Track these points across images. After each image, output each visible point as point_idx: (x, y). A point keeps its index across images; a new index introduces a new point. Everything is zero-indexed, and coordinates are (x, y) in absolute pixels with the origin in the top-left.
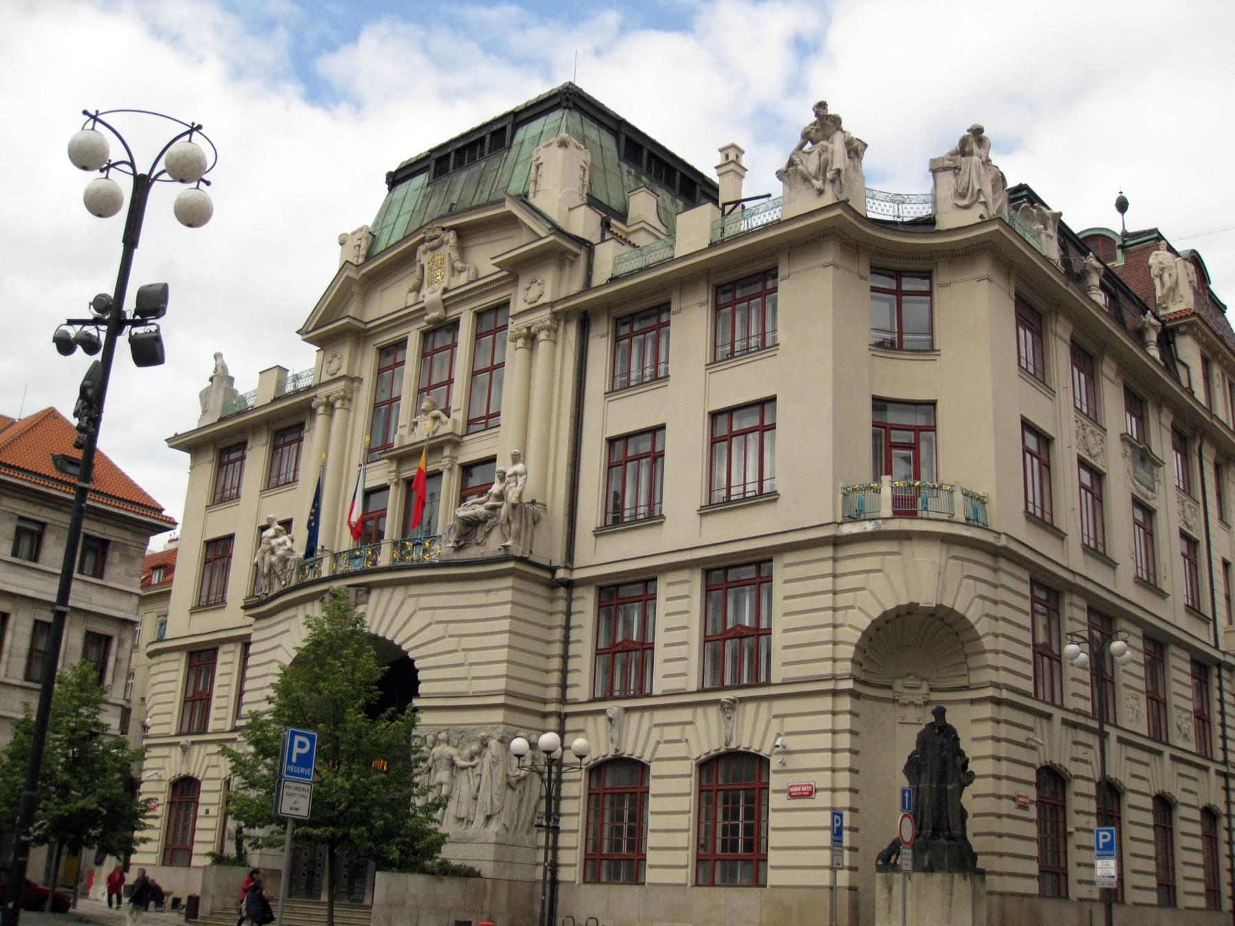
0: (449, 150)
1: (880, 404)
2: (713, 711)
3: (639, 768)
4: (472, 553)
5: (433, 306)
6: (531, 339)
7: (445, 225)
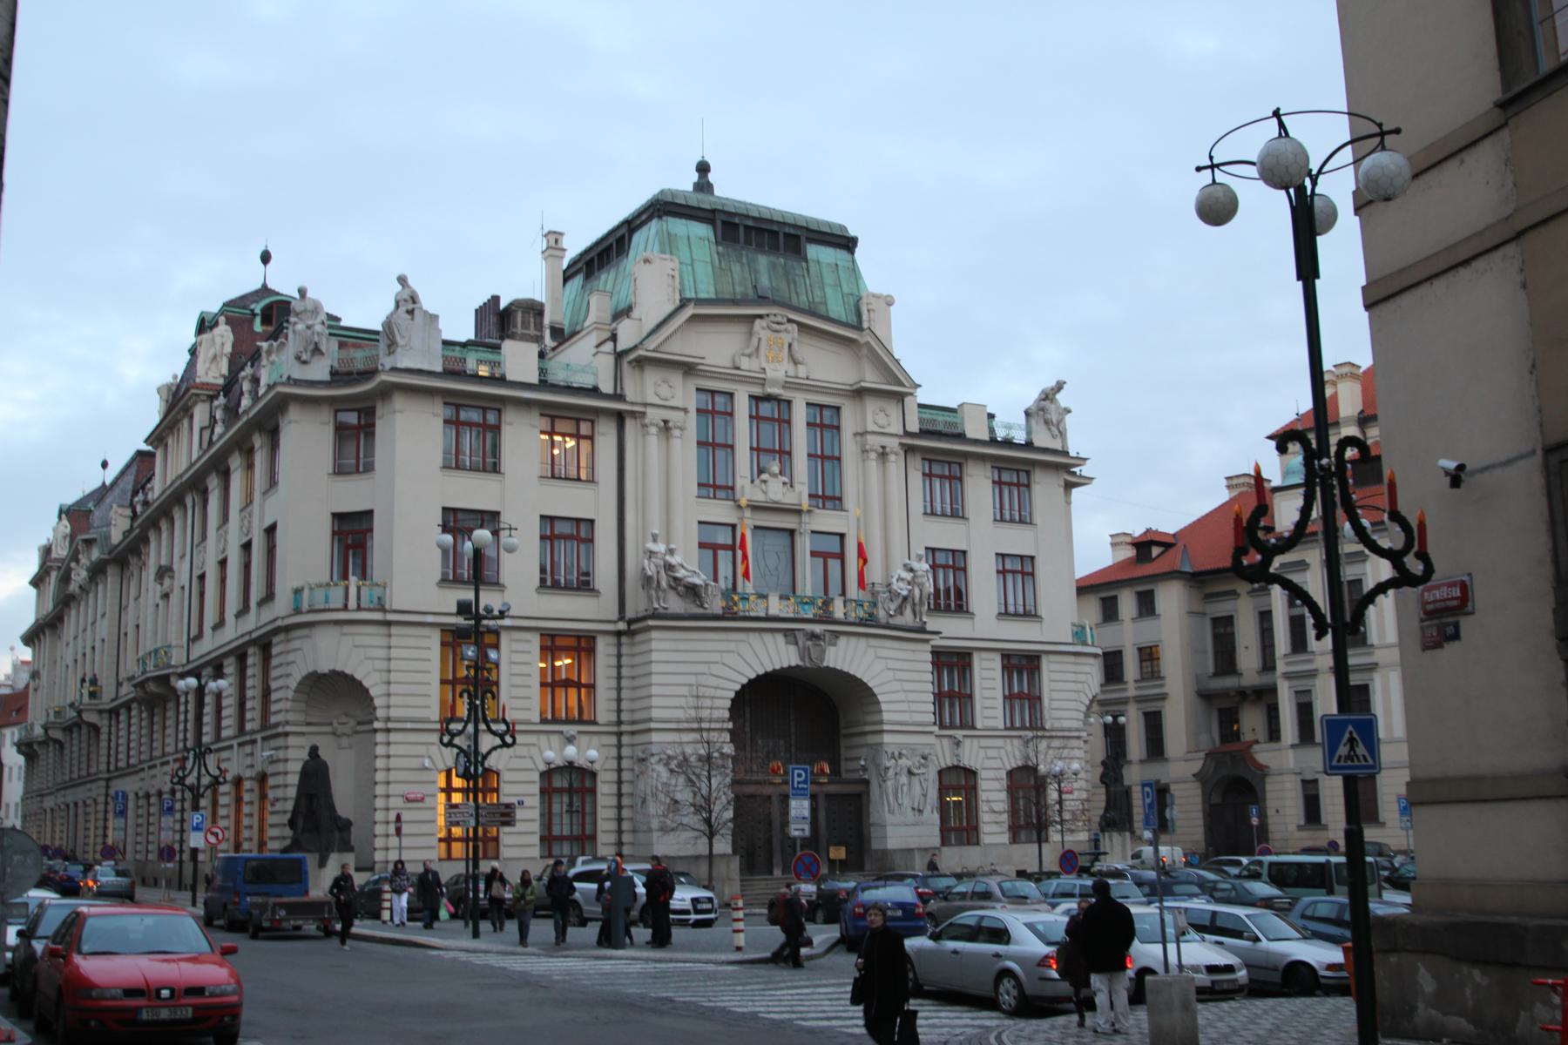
0: (737, 220)
1: (1002, 556)
2: (1016, 742)
3: (971, 773)
4: (898, 621)
5: (774, 383)
6: (883, 454)
7: (792, 316)
